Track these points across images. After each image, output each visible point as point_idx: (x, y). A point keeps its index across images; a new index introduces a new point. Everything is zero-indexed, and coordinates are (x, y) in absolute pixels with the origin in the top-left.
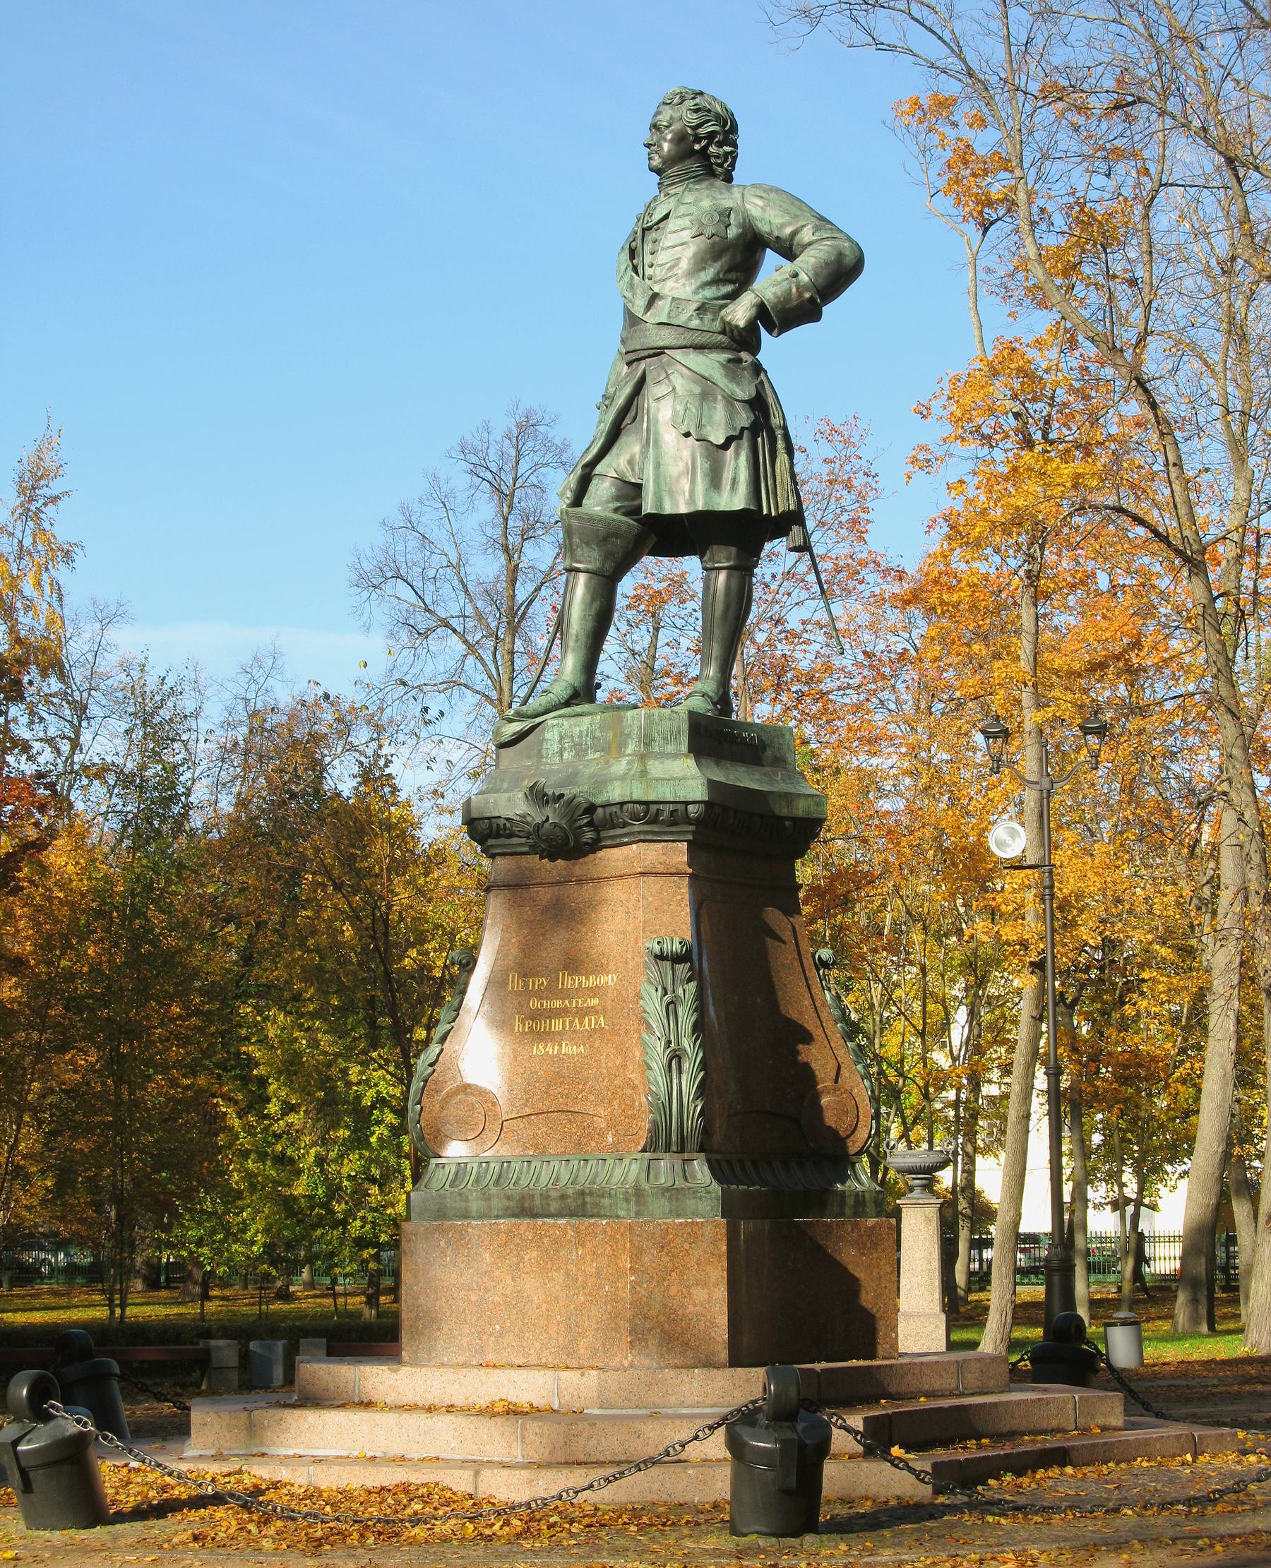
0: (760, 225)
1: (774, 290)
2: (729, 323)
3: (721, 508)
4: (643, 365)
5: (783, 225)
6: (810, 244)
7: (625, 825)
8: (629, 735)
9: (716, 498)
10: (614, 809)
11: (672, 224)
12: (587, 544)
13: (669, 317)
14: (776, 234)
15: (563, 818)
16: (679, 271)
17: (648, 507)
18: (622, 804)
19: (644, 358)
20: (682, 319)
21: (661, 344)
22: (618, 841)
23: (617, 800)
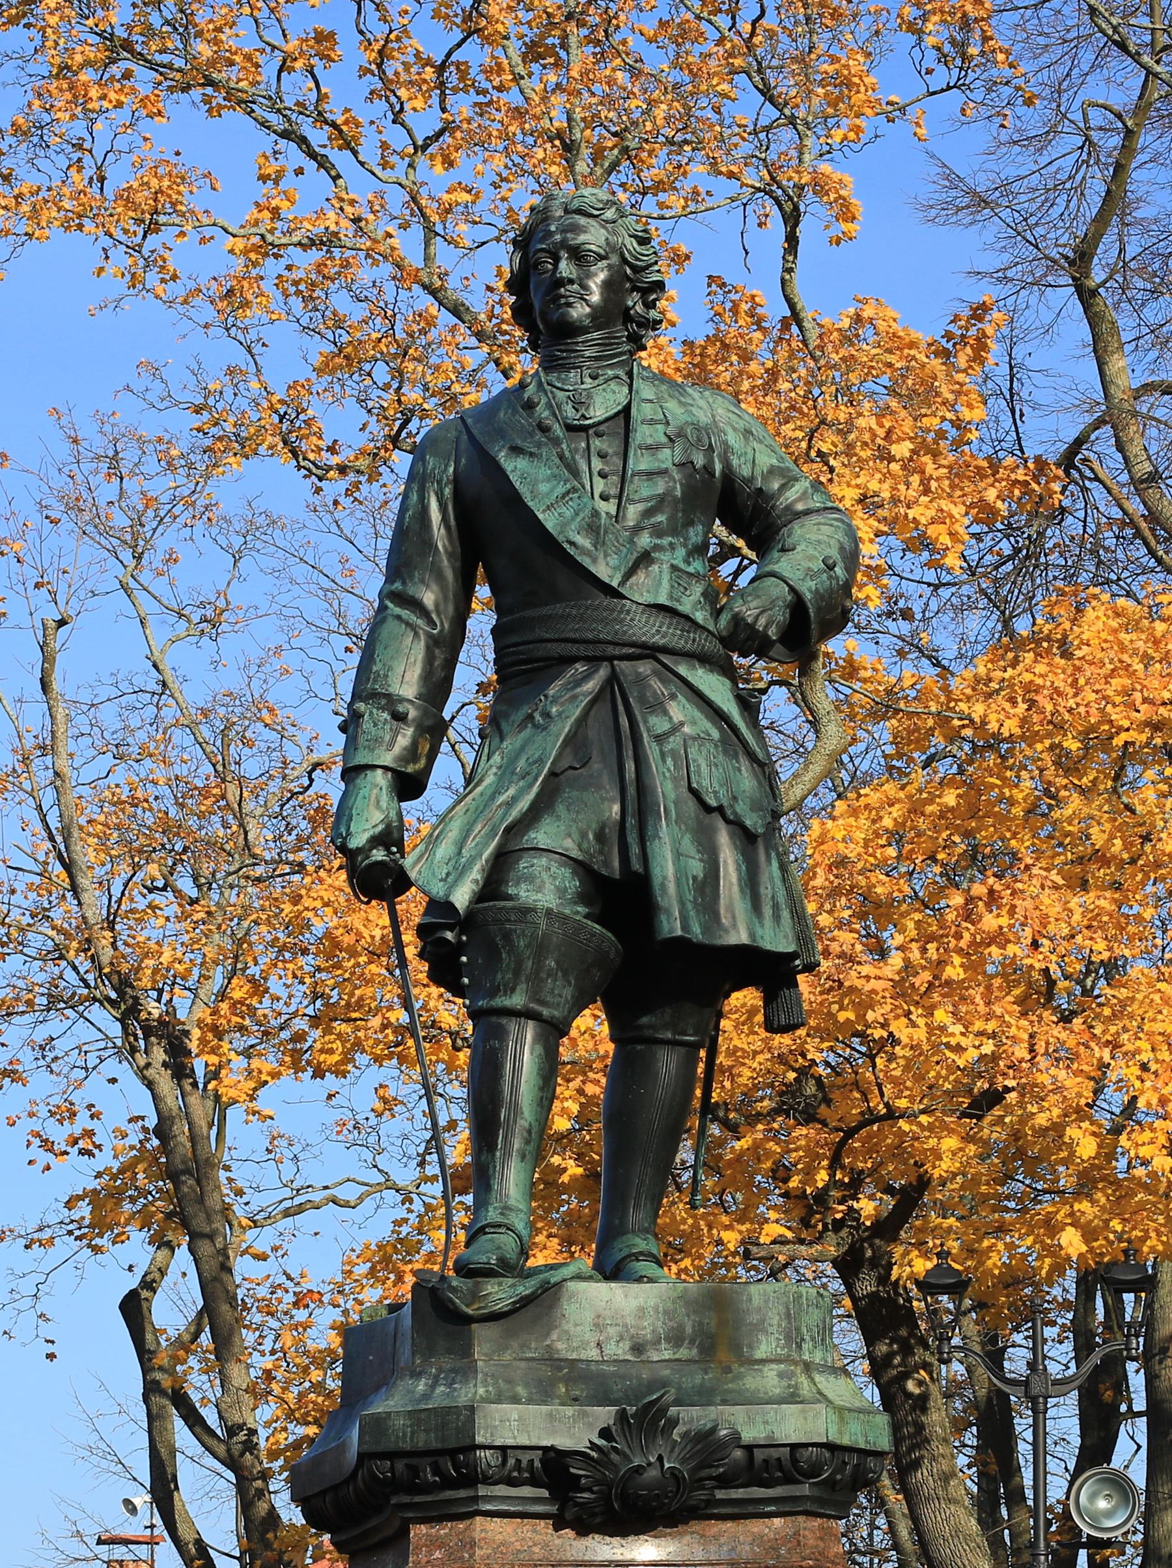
0: (735, 462)
1: (812, 584)
2: (751, 627)
3: (768, 947)
4: (603, 672)
5: (772, 471)
6: (807, 512)
7: (789, 1480)
8: (760, 1327)
9: (759, 932)
10: (774, 1453)
11: (643, 434)
12: (565, 974)
13: (671, 597)
14: (759, 483)
15: (683, 1461)
16: (661, 518)
17: (671, 925)
18: (794, 1447)
19: (610, 659)
20: (685, 607)
21: (658, 640)
22: (751, 1509)
23: (793, 1440)
